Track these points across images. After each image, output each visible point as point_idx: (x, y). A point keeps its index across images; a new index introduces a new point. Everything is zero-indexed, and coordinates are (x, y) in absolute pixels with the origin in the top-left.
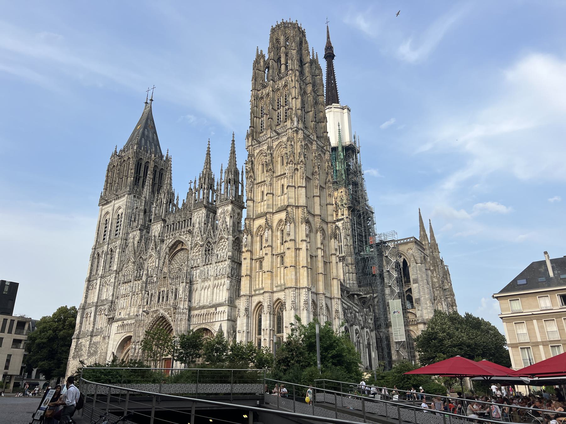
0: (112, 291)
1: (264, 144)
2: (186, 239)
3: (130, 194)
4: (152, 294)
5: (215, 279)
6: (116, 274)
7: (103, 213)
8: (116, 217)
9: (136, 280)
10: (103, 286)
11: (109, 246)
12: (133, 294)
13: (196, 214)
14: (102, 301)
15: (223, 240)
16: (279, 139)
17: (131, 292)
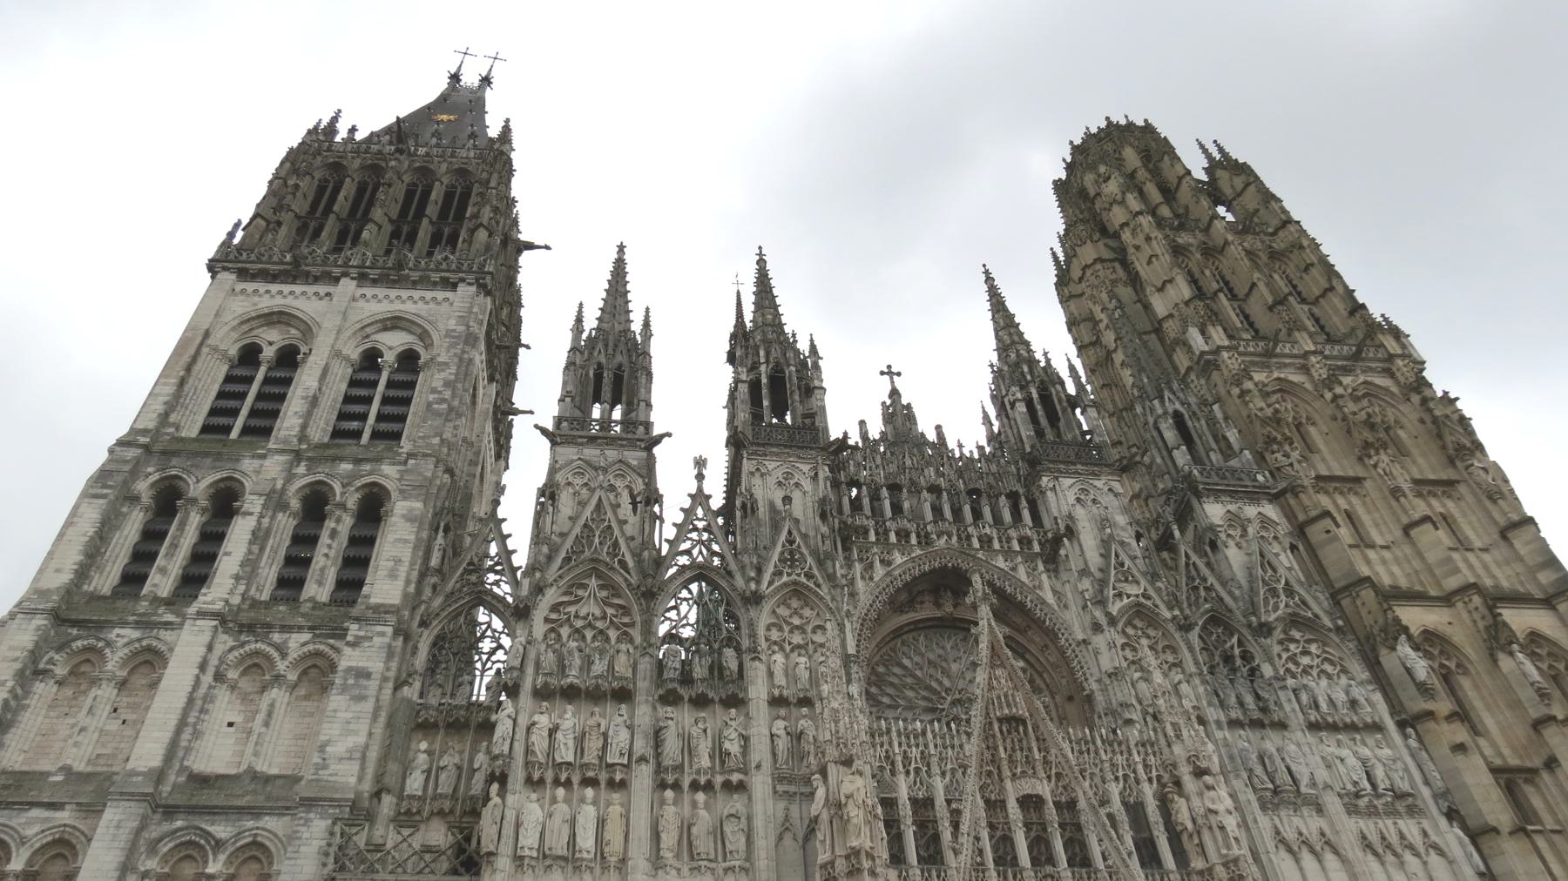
0: (364, 727)
1: (1286, 365)
2: (1024, 578)
3: (488, 293)
4: (923, 805)
5: (1352, 810)
6: (397, 632)
7: (241, 307)
8: (355, 354)
9: (671, 699)
10: (219, 677)
11: (301, 469)
12: (670, 779)
13: (1067, 482)
14: (203, 781)
15: (1296, 634)
16: (1351, 371)
17: (642, 759)
